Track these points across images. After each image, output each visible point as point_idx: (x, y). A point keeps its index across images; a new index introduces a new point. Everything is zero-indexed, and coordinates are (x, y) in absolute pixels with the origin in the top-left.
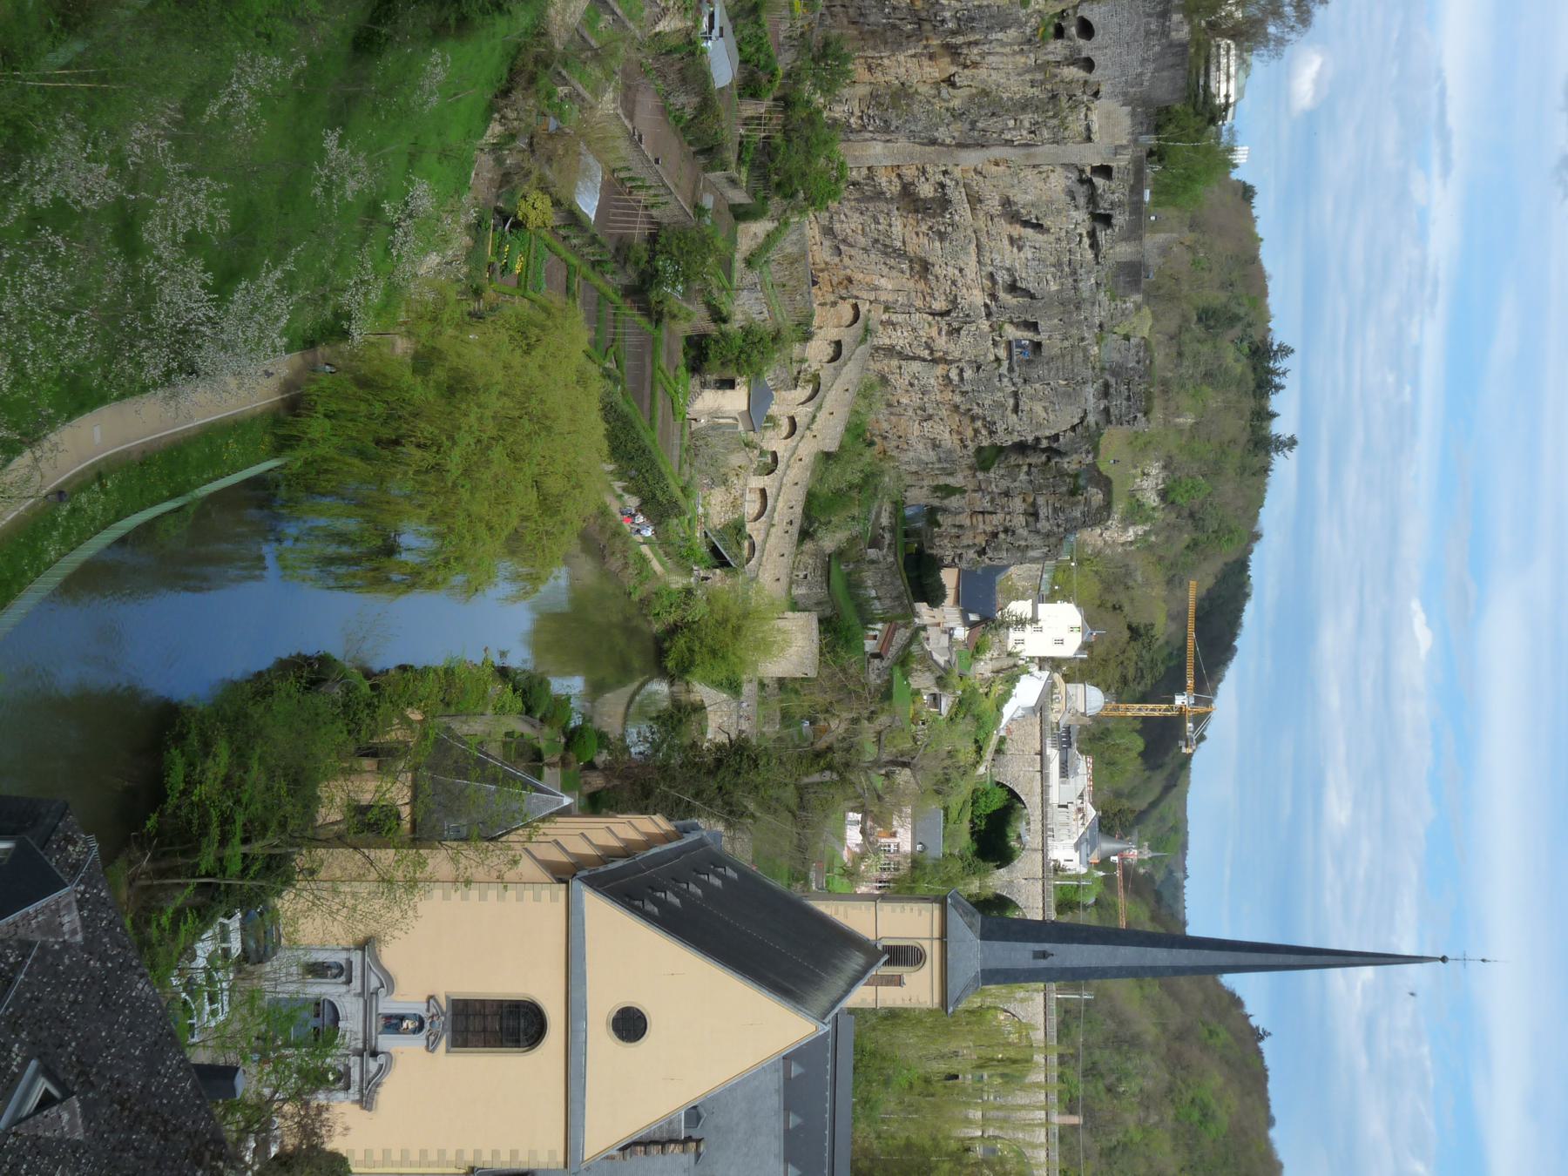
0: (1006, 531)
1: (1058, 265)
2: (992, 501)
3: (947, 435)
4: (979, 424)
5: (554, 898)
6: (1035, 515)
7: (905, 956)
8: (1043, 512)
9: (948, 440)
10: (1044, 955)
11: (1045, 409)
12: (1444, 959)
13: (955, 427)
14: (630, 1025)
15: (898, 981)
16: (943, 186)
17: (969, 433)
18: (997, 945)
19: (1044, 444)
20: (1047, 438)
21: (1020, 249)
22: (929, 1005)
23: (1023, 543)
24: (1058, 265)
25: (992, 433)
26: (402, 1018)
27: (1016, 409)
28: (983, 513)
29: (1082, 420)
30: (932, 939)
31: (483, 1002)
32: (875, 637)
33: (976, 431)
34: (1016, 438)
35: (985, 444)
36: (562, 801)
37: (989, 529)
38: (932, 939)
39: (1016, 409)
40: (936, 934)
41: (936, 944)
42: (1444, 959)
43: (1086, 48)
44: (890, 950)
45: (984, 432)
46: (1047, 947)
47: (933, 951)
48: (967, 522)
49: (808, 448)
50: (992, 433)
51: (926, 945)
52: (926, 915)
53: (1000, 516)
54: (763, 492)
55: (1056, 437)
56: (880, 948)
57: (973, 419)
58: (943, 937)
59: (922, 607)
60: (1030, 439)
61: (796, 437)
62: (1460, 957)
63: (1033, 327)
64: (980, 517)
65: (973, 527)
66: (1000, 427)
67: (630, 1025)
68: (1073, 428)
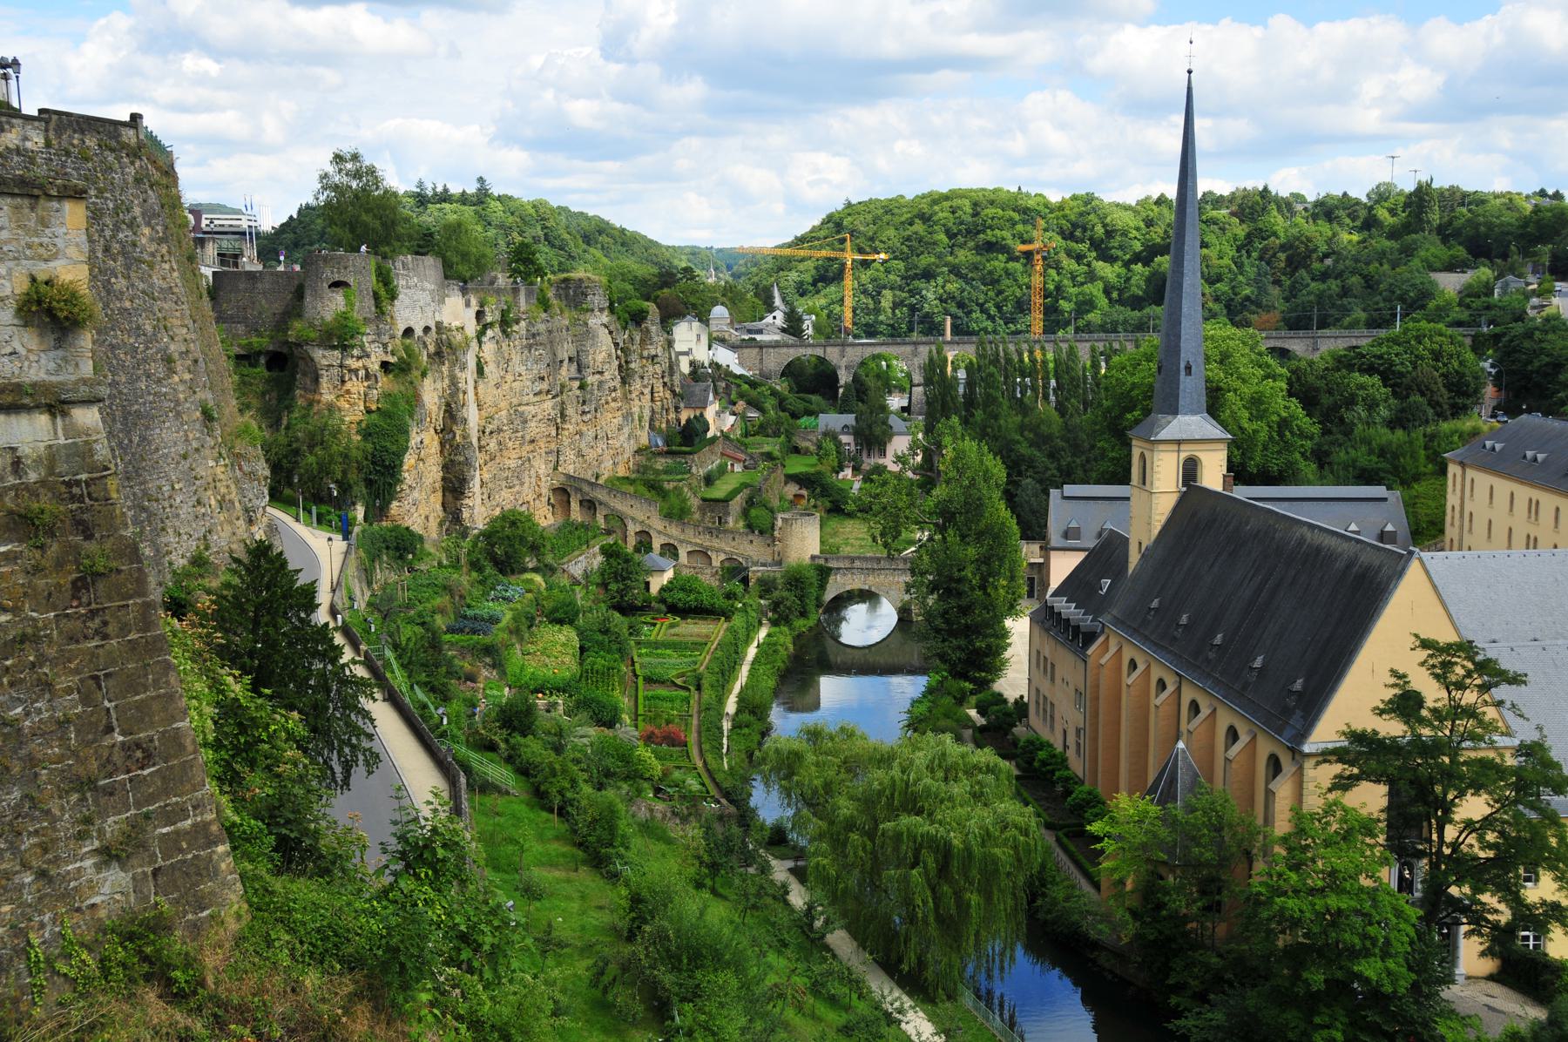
1: (530, 347)
2: (645, 387)
6: (654, 357)
7: (1190, 470)
8: (653, 352)
9: (618, 420)
10: (1188, 369)
12: (1190, 72)
16: (491, 433)
17: (613, 404)
18: (1181, 402)
21: (520, 375)
24: (530, 347)
25: (615, 390)
26: (1401, 878)
27: (601, 373)
28: (652, 393)
29: (606, 327)
30: (1179, 451)
32: (732, 465)
33: (614, 400)
35: (619, 393)
36: (1183, 750)
38: (1179, 451)
39: (601, 373)
40: (1175, 447)
41: (1183, 447)
42: (1190, 72)
43: (419, 332)
45: (613, 395)
46: (1182, 365)
51: (1183, 455)
52: (1163, 455)
54: (689, 553)
55: (616, 345)
56: (1184, 489)
59: (710, 435)
62: (1187, 59)
63: (561, 362)
66: (612, 384)
68: (611, 333)
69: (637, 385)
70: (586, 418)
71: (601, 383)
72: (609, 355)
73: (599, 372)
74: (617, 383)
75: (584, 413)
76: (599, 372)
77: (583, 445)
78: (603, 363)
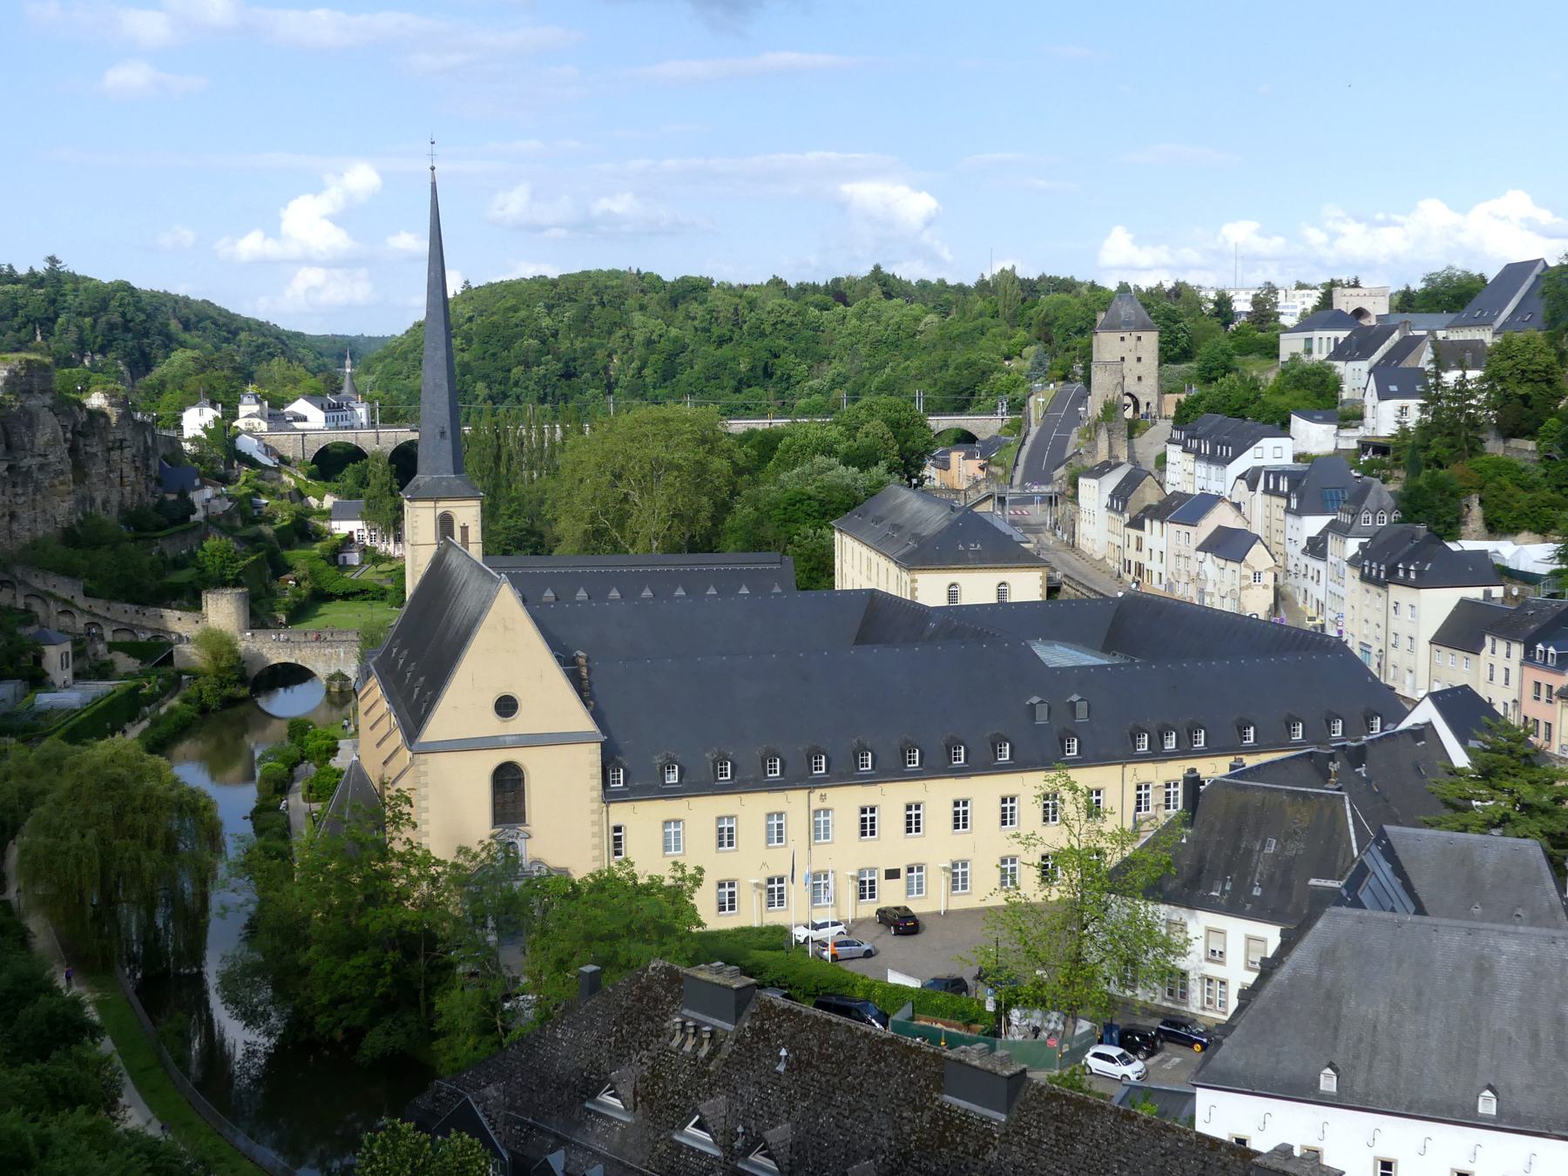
0: (134, 461)
3: (65, 505)
4: (56, 482)
5: (425, 763)
7: (445, 523)
11: (43, 435)
12: (433, 169)
13: (59, 499)
14: (506, 706)
15: (465, 529)
17: (61, 488)
19: (69, 435)
20: (65, 433)
22: (479, 509)
23: (142, 449)
25: (62, 473)
28: (122, 478)
31: (495, 804)
33: (62, 483)
34: (66, 455)
37: (133, 474)
40: (432, 504)
42: (433, 169)
44: (443, 538)
45: (61, 478)
47: (443, 506)
48: (129, 488)
49: (81, 602)
50: (62, 473)
51: (439, 511)
53: (124, 465)
57: (52, 486)
58: (437, 500)
60: (68, 445)
61: (73, 610)
64: (125, 480)
65: (132, 484)
67: (506, 706)
68: (56, 415)
69: (97, 469)
70: (21, 500)
71: (41, 467)
72: (55, 439)
73: (40, 455)
74: (67, 465)
75: (16, 495)
76: (40, 455)
77: (15, 527)
78: (47, 444)
